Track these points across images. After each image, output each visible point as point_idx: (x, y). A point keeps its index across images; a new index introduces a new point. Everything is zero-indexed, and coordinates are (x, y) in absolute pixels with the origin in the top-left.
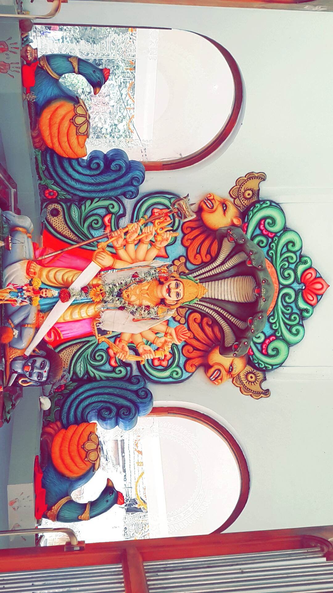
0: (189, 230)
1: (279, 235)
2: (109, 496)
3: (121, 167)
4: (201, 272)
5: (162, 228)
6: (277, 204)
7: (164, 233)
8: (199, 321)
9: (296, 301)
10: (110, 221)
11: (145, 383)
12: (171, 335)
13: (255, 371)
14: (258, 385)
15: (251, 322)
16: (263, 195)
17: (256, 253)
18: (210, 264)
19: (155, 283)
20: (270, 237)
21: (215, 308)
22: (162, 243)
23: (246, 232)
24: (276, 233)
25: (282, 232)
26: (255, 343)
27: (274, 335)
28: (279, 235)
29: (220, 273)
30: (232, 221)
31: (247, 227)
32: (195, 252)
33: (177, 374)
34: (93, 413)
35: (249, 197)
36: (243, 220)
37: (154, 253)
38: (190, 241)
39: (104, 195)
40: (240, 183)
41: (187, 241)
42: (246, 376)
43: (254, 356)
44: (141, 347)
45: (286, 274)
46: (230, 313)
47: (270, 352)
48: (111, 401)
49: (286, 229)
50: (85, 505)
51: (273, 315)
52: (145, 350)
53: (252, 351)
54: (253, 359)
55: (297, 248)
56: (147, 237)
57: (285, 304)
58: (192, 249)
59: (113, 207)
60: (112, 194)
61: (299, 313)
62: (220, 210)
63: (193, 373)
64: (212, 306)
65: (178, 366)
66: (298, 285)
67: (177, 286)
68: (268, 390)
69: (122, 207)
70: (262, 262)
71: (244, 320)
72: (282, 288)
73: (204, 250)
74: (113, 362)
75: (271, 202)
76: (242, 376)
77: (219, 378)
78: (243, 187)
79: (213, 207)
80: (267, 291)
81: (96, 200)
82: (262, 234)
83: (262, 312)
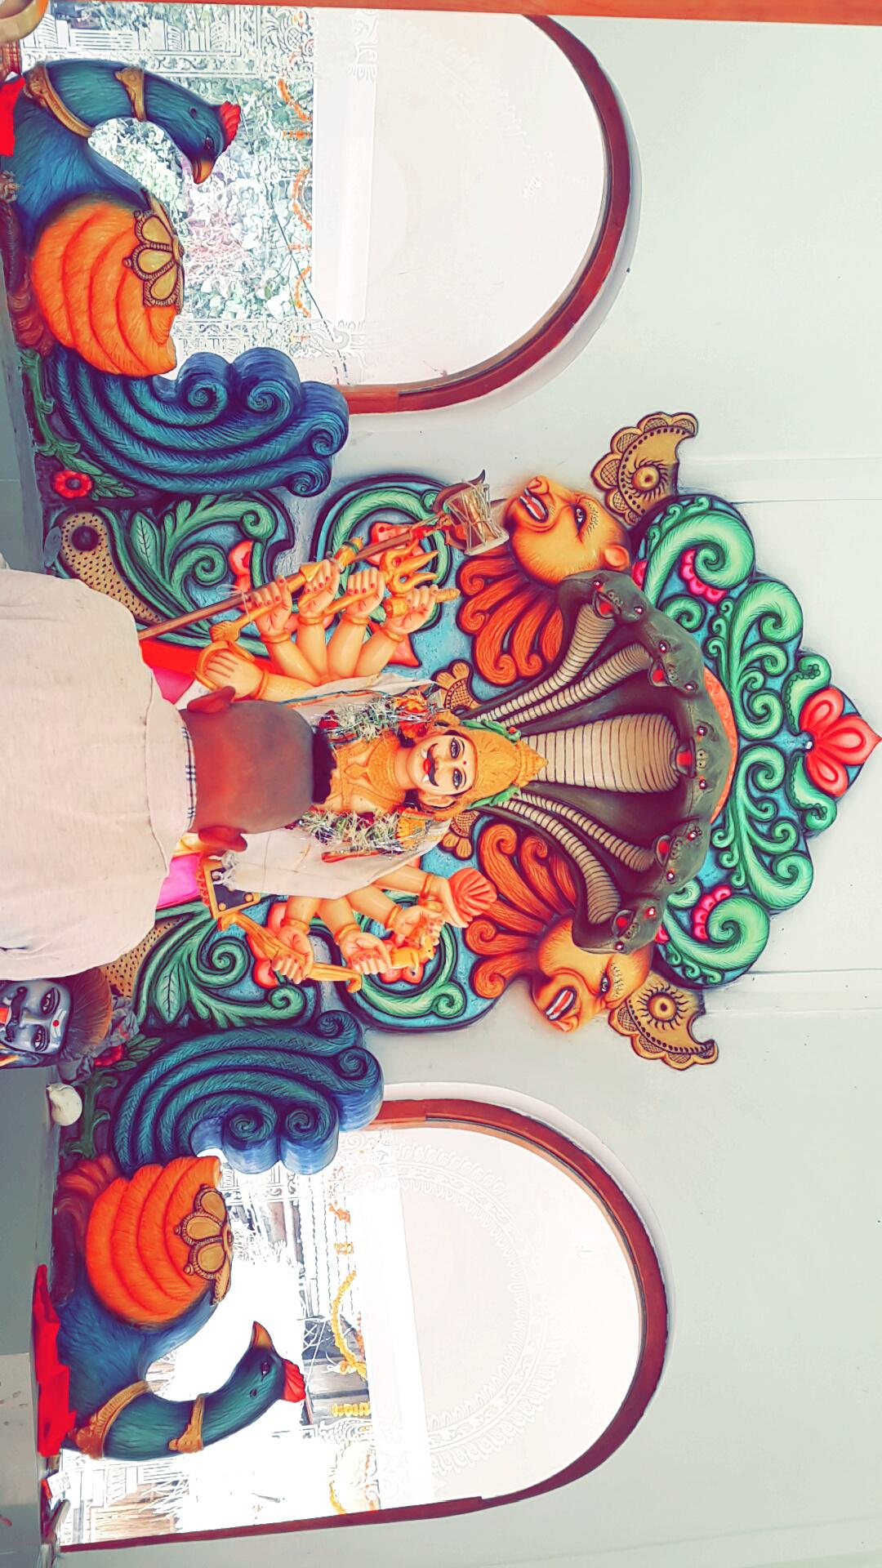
0: (478, 584)
1: (735, 594)
2: (259, 1377)
3: (277, 402)
4: (516, 704)
5: (407, 577)
6: (730, 505)
7: (411, 590)
8: (510, 848)
9: (786, 784)
10: (248, 561)
11: (359, 1033)
12: (438, 899)
13: (673, 988)
14: (683, 1028)
15: (667, 852)
16: (688, 480)
17: (677, 648)
18: (541, 682)
19: (388, 743)
20: (710, 602)
21: (558, 809)
22: (408, 622)
23: (643, 586)
24: (728, 590)
25: (744, 585)
26: (673, 909)
28: (735, 594)
29: (570, 708)
30: (602, 557)
31: (645, 573)
32: (498, 649)
33: (451, 1004)
34: (207, 1128)
35: (647, 490)
36: (634, 552)
37: (384, 651)
38: (481, 618)
39: (228, 485)
40: (624, 443)
42: (649, 1003)
43: (670, 947)
44: (350, 938)
45: (757, 706)
46: (600, 824)
47: (716, 932)
48: (261, 1089)
49: (754, 578)
50: (189, 1406)
51: (723, 826)
52: (362, 949)
53: (665, 931)
54: (668, 955)
55: (787, 631)
56: (361, 603)
57: (756, 794)
58: (488, 640)
59: (257, 521)
60: (252, 481)
62: (567, 524)
63: (496, 999)
64: (549, 806)
65: (452, 980)
67: (455, 751)
68: (712, 1042)
69: (281, 520)
70: (695, 673)
71: (643, 842)
72: (747, 749)
73: (522, 645)
74: (264, 976)
75: (713, 498)
76: (637, 1005)
77: (573, 1012)
78: (632, 458)
80: (712, 760)
81: (204, 502)
82: (688, 594)
83: (696, 818)
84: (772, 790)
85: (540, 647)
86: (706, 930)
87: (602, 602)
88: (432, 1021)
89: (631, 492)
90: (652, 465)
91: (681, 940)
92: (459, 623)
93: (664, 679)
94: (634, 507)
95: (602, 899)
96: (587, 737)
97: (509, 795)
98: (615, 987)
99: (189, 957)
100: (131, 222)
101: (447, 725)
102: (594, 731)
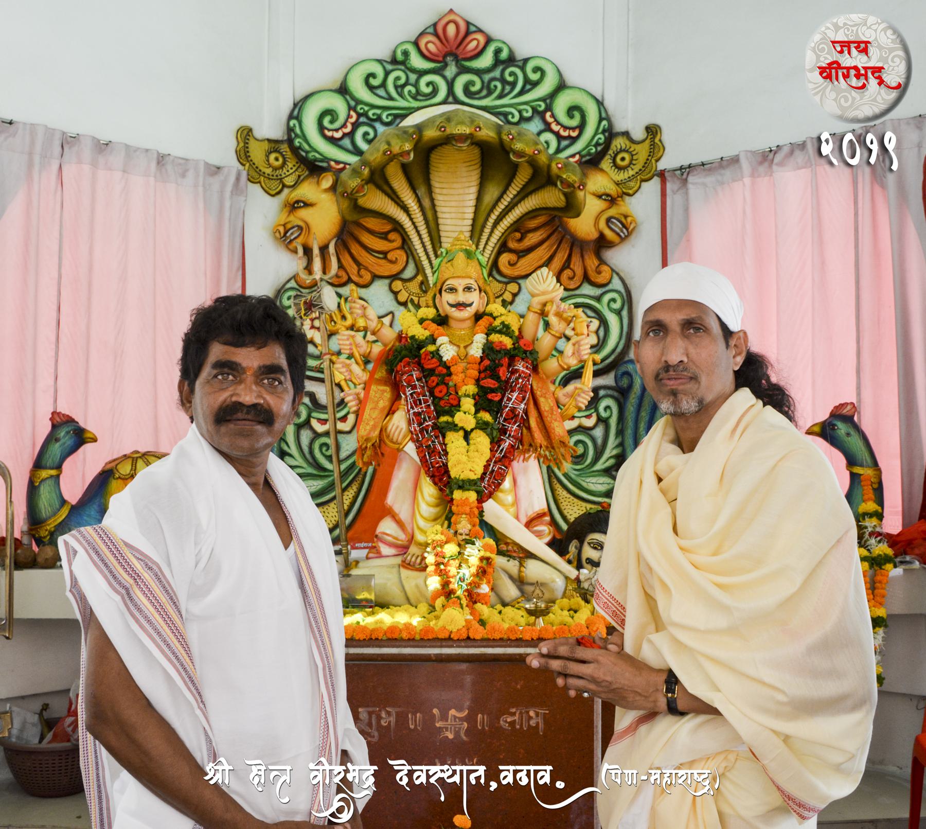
1: (353, 103)
6: (295, 105)
8: (513, 257)
9: (478, 72)
10: (323, 422)
12: (545, 305)
13: (611, 152)
14: (638, 148)
15: (520, 154)
17: (389, 144)
18: (406, 233)
24: (350, 108)
25: (348, 97)
26: (559, 150)
27: (542, 115)
28: (353, 103)
30: (326, 190)
31: (338, 162)
33: (614, 300)
35: (281, 160)
36: (322, 170)
38: (363, 272)
41: (361, 277)
43: (584, 153)
47: (575, 122)
51: (505, 115)
52: (574, 353)
53: (573, 156)
55: (379, 71)
57: (484, 93)
58: (378, 268)
61: (501, 67)
62: (304, 214)
63: (613, 270)
65: (598, 299)
66: (448, 68)
71: (515, 168)
75: (291, 117)
76: (622, 176)
77: (623, 220)
78: (263, 170)
79: (300, 228)
80: (462, 123)
81: (285, 448)
82: (351, 135)
84: (483, 82)
85: (383, 233)
86: (573, 129)
87: (357, 192)
88: (625, 313)
89: (285, 170)
90: (267, 156)
91: (579, 146)
92: (365, 286)
93: (408, 153)
94: (294, 169)
95: (551, 198)
96: (443, 204)
97: (480, 257)
98: (608, 191)
99: (575, 470)
100: (120, 481)
101: (435, 295)
102: (439, 199)
